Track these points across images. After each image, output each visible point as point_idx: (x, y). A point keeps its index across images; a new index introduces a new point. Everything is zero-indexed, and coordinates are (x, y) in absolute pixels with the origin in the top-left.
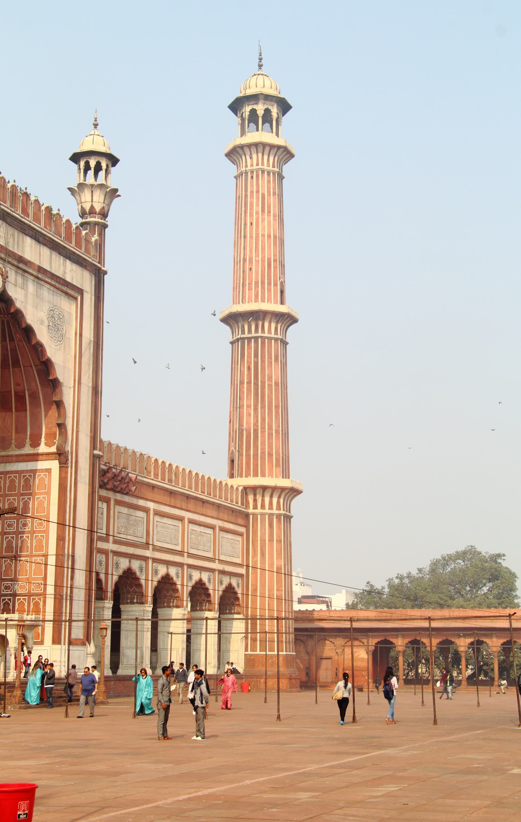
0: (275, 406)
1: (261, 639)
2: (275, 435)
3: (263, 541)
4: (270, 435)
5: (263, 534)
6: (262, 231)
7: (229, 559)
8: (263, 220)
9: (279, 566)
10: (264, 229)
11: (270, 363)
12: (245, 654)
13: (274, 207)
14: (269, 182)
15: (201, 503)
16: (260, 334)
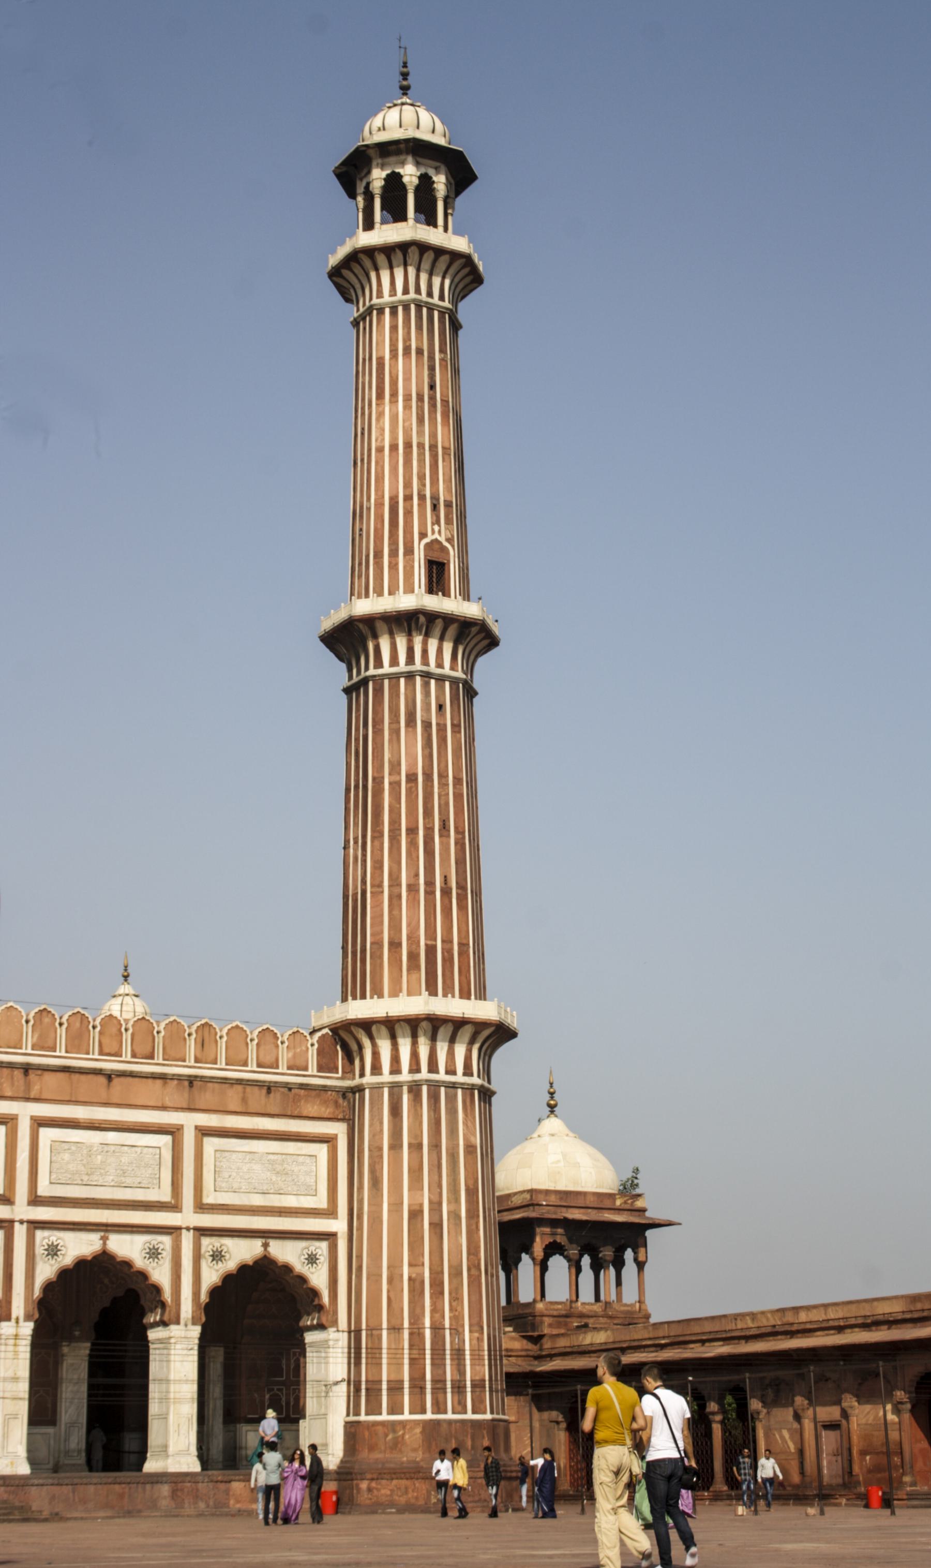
0: (407, 830)
1: (369, 1386)
2: (408, 896)
3: (376, 1150)
4: (395, 898)
5: (376, 1134)
6: (376, 440)
7: (257, 1200)
8: (381, 415)
9: (417, 1208)
10: (383, 434)
11: (395, 732)
12: (346, 1423)
13: (407, 379)
14: (394, 328)
15: (102, 1080)
16: (372, 672)
